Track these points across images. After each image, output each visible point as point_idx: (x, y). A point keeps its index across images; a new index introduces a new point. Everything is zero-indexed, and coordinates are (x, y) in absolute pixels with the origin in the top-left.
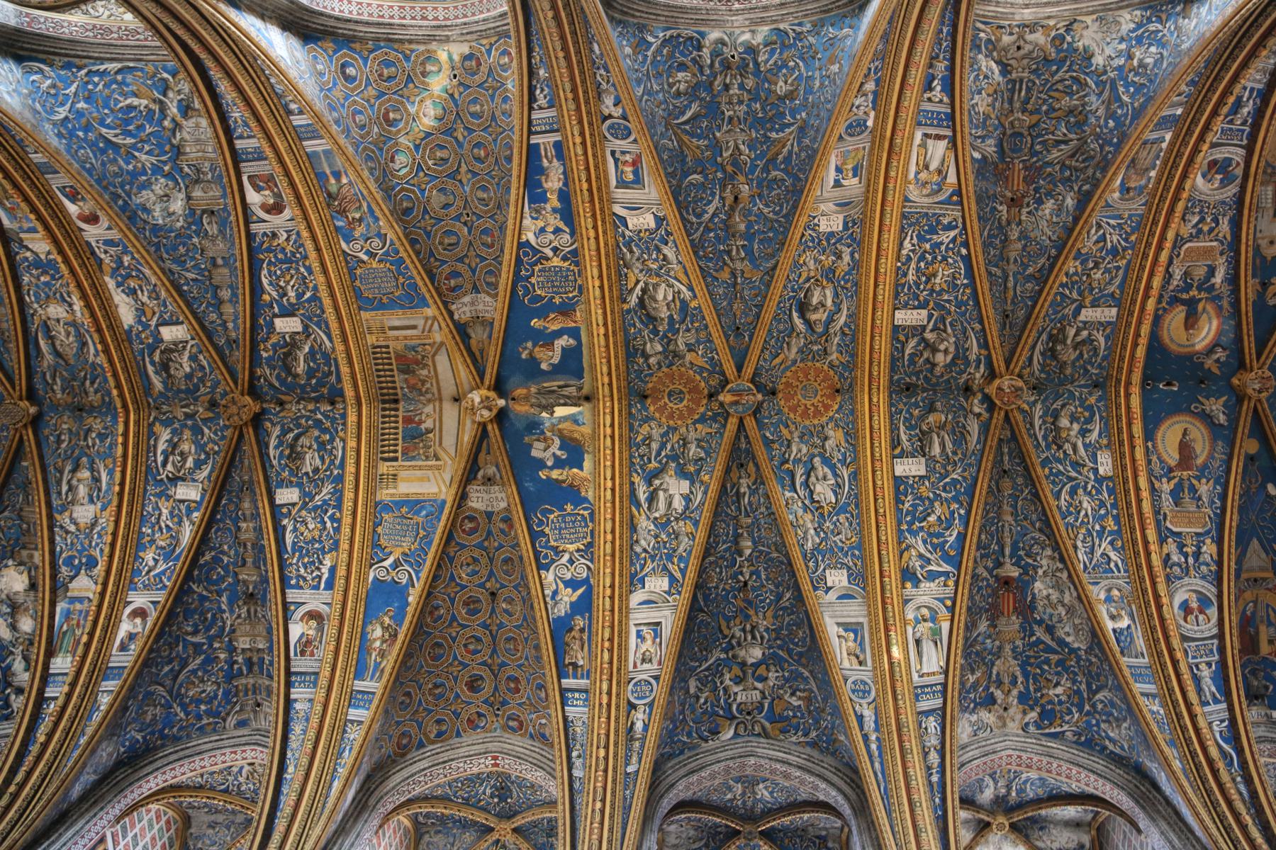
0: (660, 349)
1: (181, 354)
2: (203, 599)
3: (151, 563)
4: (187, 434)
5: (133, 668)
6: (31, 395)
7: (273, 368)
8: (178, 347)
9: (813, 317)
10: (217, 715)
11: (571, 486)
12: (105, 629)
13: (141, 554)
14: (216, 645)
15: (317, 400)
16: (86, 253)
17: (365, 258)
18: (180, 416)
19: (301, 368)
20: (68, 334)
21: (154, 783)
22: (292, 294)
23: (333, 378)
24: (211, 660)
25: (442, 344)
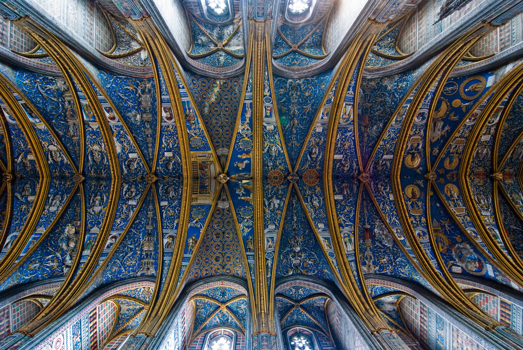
0: (272, 164)
1: (134, 162)
2: (135, 234)
3: (119, 223)
4: (133, 186)
6: (84, 174)
7: (162, 167)
8: (134, 160)
9: (313, 156)
11: (247, 201)
12: (103, 241)
14: (137, 249)
15: (174, 177)
16: (110, 129)
17: (194, 135)
18: (131, 181)
19: (171, 167)
20: (99, 155)
22: (171, 145)
23: (180, 171)
24: (135, 253)
25: (213, 161)
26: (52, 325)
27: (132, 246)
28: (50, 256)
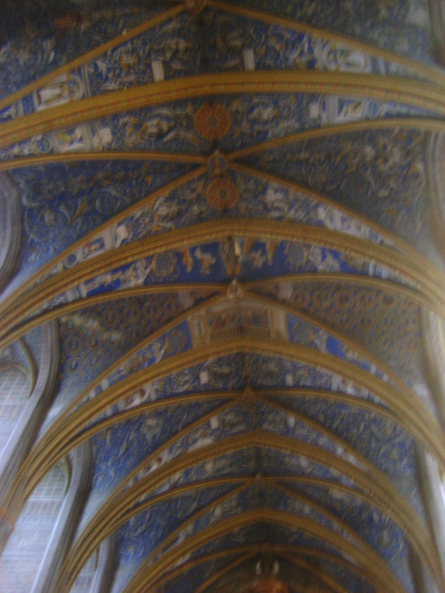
16: (176, 461)
24: (374, 420)
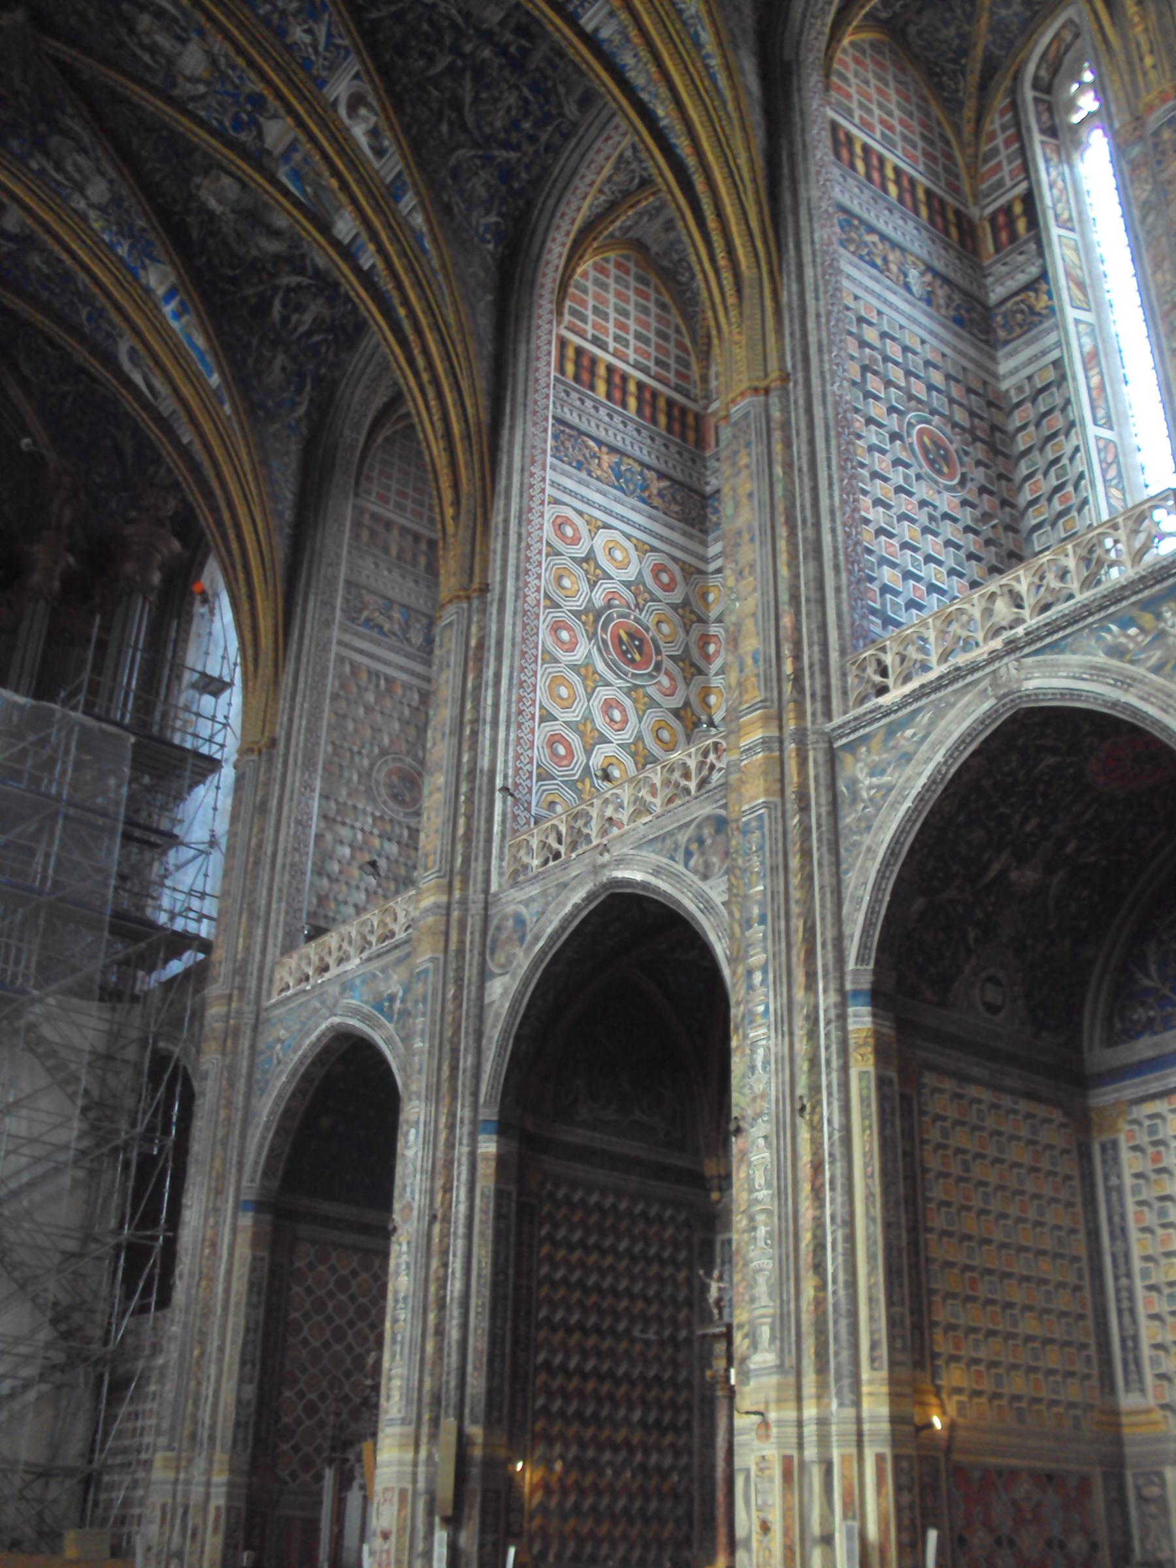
2: (398, 17)
3: (307, 39)
5: (407, 165)
10: (547, 118)
12: (342, 152)
13: (289, 40)
14: (468, 48)
21: (557, 249)
24: (480, 72)
26: (500, 518)
27: (443, 62)
28: (277, 306)
